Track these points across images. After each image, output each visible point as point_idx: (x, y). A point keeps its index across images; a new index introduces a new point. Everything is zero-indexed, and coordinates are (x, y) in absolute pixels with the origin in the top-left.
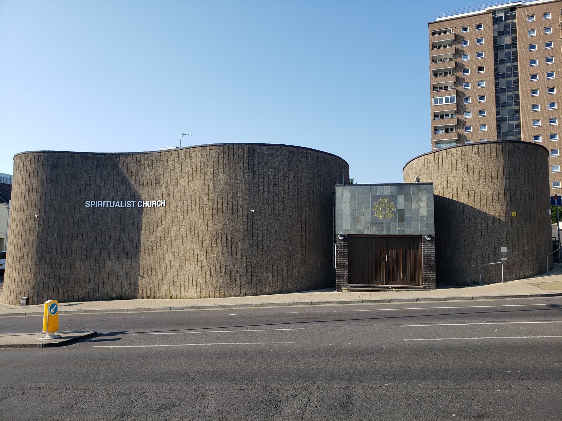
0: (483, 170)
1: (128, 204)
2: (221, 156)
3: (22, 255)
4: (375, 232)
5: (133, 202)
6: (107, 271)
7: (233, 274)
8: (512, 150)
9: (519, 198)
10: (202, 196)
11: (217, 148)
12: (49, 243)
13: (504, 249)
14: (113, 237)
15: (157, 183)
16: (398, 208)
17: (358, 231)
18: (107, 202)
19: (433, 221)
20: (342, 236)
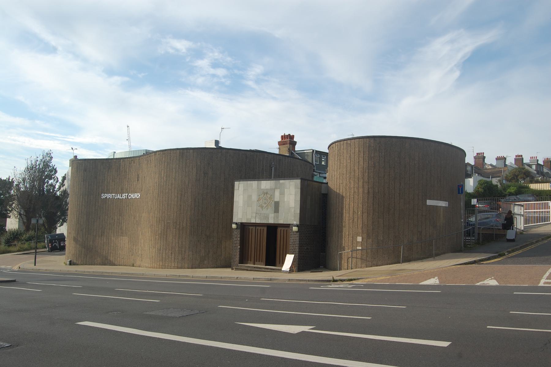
0: (349, 164)
1: (124, 196)
2: (164, 159)
4: (258, 221)
6: (112, 245)
7: (167, 252)
8: (372, 145)
9: (377, 191)
11: (162, 153)
13: (359, 239)
15: (138, 180)
16: (276, 200)
17: (247, 219)
19: (298, 211)
20: (236, 224)
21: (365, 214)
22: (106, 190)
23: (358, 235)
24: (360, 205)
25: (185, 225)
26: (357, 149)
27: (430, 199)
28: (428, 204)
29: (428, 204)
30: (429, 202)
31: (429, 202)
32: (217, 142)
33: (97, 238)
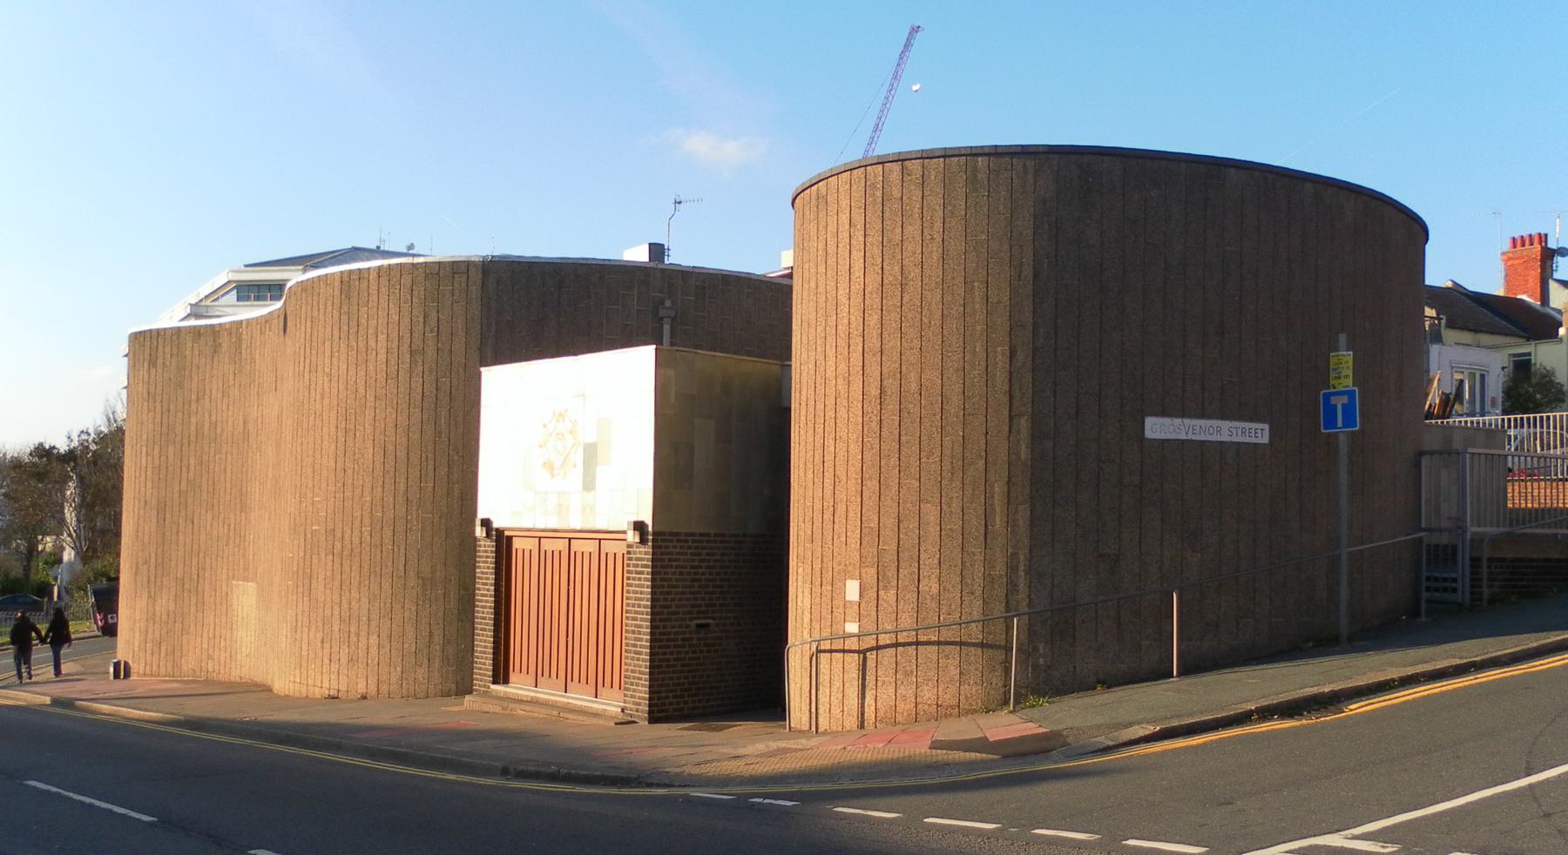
9: (914, 387)
13: (852, 590)
21: (872, 485)
23: (847, 575)
24: (855, 449)
25: (356, 541)
26: (844, 218)
27: (1164, 413)
28: (1149, 434)
29: (1149, 434)
30: (1157, 428)
31: (1157, 428)
32: (657, 250)
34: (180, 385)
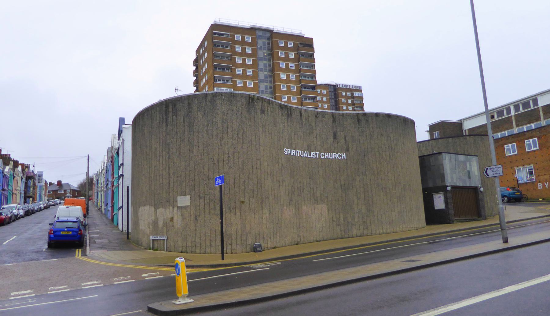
3: (242, 199)
5: (317, 153)
6: (304, 216)
10: (381, 152)
12: (266, 187)
14: (305, 184)
18: (298, 151)
22: (287, 143)
33: (285, 207)
34: (276, 126)
